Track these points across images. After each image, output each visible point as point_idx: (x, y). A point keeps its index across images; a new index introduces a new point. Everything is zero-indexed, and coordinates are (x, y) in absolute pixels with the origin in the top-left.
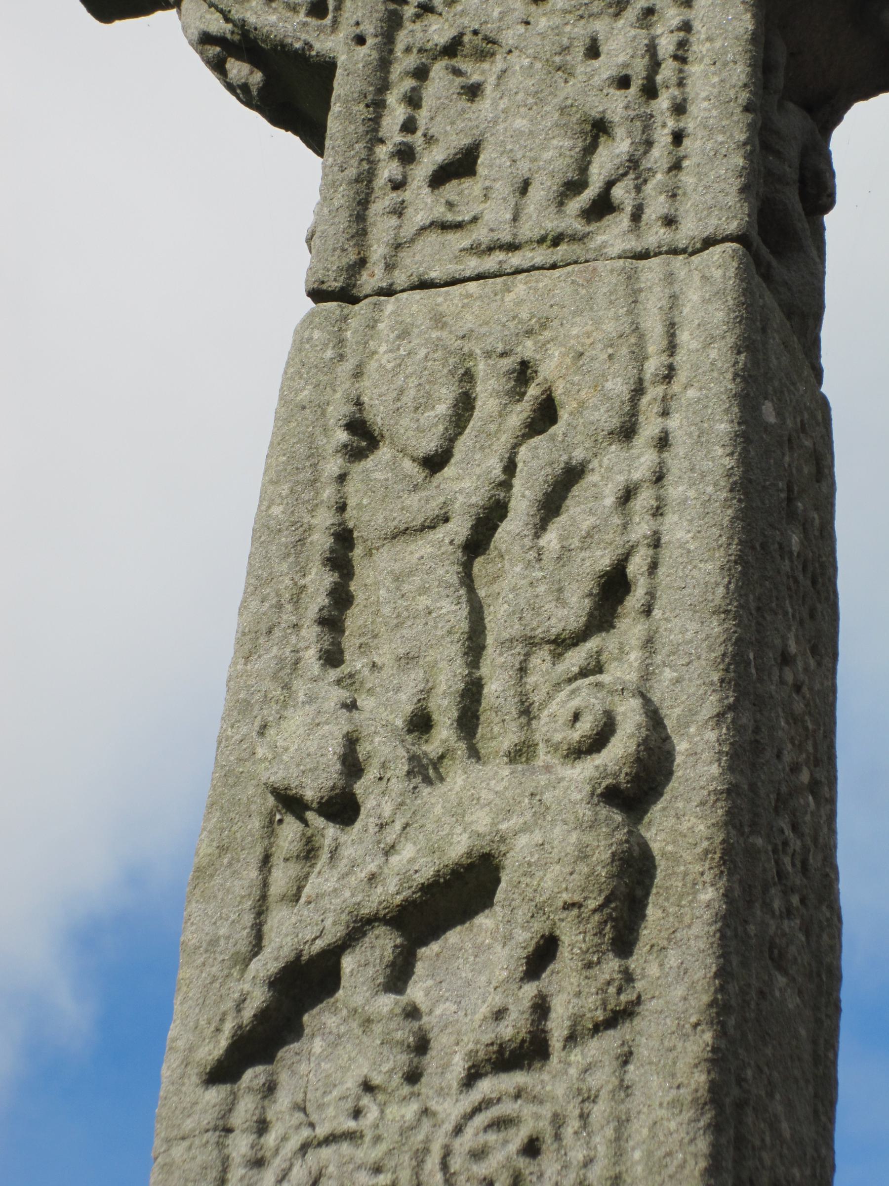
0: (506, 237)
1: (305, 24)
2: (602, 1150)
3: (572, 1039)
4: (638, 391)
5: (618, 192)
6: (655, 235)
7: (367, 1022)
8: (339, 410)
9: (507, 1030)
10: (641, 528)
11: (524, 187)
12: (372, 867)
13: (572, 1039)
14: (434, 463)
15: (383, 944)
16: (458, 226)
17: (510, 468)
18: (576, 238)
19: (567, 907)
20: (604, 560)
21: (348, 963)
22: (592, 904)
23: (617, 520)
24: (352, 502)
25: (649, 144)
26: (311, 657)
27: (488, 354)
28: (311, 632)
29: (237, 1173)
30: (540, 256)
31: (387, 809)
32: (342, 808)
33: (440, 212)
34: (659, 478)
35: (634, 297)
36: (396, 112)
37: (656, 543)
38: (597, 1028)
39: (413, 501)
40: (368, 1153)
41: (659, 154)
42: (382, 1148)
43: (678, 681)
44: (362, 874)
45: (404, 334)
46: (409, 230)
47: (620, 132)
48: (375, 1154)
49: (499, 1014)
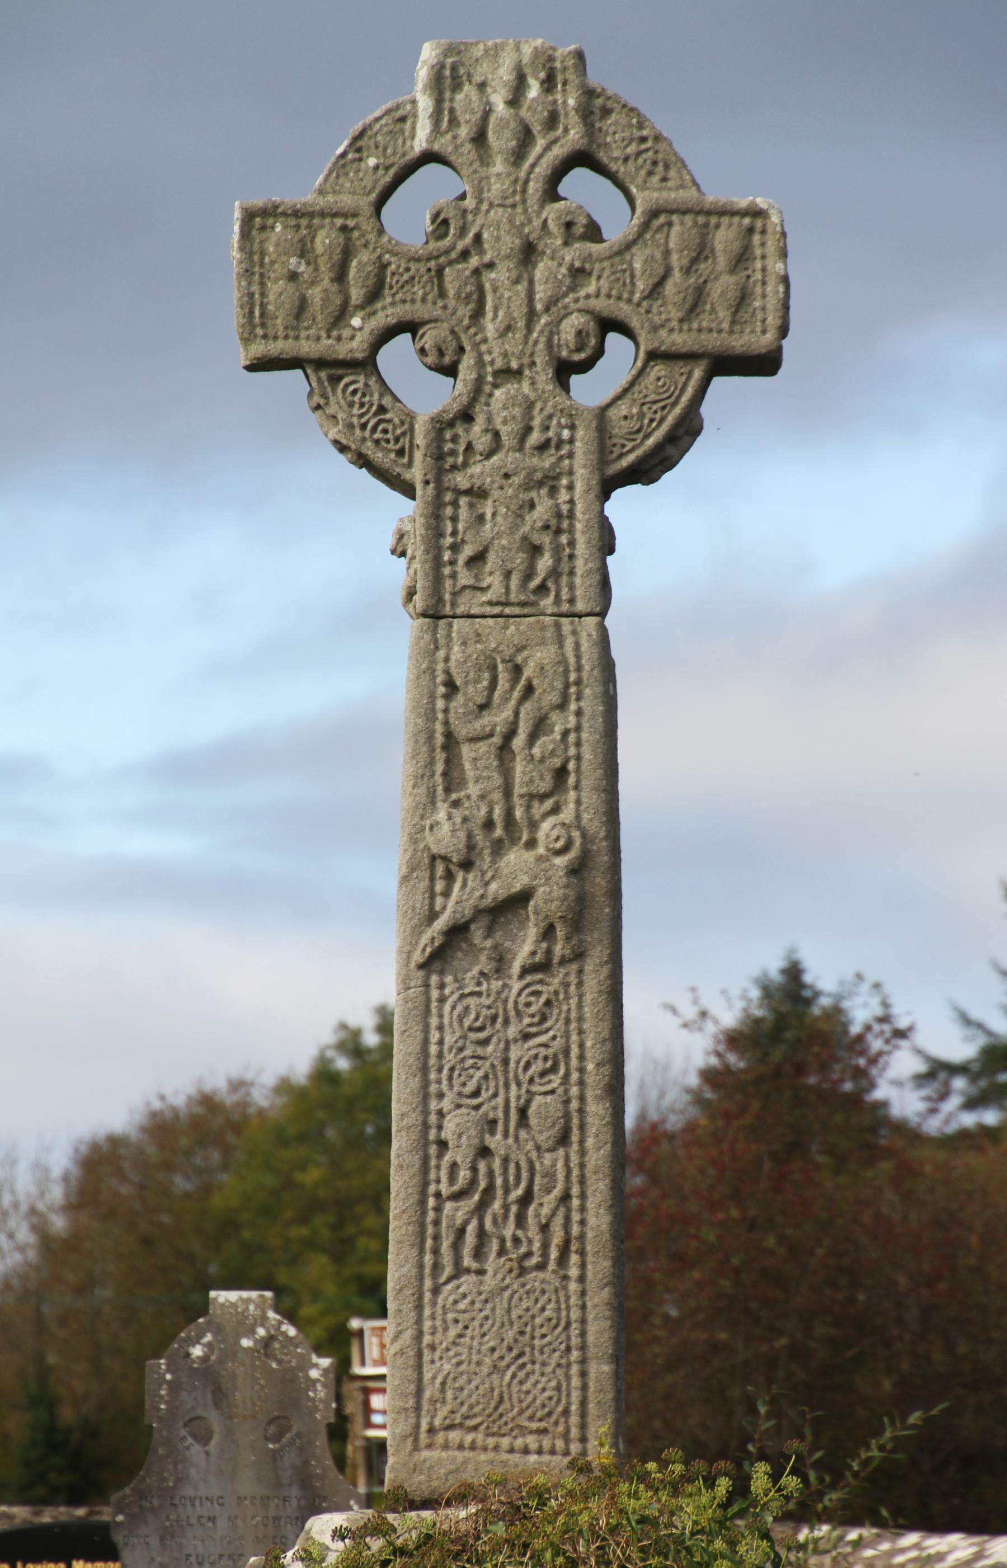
0: (503, 599)
1: (395, 461)
2: (573, 1006)
4: (567, 686)
6: (565, 607)
8: (440, 678)
9: (538, 958)
10: (572, 751)
11: (508, 575)
12: (481, 892)
14: (483, 707)
15: (485, 920)
17: (517, 714)
19: (560, 917)
20: (557, 762)
21: (473, 927)
23: (562, 747)
24: (451, 720)
26: (440, 789)
28: (438, 779)
29: (434, 1005)
30: (517, 610)
32: (467, 865)
33: (471, 581)
34: (578, 728)
36: (449, 527)
37: (578, 758)
38: (570, 961)
40: (485, 1001)
42: (492, 999)
43: (591, 820)
44: (478, 894)
45: (464, 643)
46: (457, 588)
48: (488, 1002)
49: (533, 953)
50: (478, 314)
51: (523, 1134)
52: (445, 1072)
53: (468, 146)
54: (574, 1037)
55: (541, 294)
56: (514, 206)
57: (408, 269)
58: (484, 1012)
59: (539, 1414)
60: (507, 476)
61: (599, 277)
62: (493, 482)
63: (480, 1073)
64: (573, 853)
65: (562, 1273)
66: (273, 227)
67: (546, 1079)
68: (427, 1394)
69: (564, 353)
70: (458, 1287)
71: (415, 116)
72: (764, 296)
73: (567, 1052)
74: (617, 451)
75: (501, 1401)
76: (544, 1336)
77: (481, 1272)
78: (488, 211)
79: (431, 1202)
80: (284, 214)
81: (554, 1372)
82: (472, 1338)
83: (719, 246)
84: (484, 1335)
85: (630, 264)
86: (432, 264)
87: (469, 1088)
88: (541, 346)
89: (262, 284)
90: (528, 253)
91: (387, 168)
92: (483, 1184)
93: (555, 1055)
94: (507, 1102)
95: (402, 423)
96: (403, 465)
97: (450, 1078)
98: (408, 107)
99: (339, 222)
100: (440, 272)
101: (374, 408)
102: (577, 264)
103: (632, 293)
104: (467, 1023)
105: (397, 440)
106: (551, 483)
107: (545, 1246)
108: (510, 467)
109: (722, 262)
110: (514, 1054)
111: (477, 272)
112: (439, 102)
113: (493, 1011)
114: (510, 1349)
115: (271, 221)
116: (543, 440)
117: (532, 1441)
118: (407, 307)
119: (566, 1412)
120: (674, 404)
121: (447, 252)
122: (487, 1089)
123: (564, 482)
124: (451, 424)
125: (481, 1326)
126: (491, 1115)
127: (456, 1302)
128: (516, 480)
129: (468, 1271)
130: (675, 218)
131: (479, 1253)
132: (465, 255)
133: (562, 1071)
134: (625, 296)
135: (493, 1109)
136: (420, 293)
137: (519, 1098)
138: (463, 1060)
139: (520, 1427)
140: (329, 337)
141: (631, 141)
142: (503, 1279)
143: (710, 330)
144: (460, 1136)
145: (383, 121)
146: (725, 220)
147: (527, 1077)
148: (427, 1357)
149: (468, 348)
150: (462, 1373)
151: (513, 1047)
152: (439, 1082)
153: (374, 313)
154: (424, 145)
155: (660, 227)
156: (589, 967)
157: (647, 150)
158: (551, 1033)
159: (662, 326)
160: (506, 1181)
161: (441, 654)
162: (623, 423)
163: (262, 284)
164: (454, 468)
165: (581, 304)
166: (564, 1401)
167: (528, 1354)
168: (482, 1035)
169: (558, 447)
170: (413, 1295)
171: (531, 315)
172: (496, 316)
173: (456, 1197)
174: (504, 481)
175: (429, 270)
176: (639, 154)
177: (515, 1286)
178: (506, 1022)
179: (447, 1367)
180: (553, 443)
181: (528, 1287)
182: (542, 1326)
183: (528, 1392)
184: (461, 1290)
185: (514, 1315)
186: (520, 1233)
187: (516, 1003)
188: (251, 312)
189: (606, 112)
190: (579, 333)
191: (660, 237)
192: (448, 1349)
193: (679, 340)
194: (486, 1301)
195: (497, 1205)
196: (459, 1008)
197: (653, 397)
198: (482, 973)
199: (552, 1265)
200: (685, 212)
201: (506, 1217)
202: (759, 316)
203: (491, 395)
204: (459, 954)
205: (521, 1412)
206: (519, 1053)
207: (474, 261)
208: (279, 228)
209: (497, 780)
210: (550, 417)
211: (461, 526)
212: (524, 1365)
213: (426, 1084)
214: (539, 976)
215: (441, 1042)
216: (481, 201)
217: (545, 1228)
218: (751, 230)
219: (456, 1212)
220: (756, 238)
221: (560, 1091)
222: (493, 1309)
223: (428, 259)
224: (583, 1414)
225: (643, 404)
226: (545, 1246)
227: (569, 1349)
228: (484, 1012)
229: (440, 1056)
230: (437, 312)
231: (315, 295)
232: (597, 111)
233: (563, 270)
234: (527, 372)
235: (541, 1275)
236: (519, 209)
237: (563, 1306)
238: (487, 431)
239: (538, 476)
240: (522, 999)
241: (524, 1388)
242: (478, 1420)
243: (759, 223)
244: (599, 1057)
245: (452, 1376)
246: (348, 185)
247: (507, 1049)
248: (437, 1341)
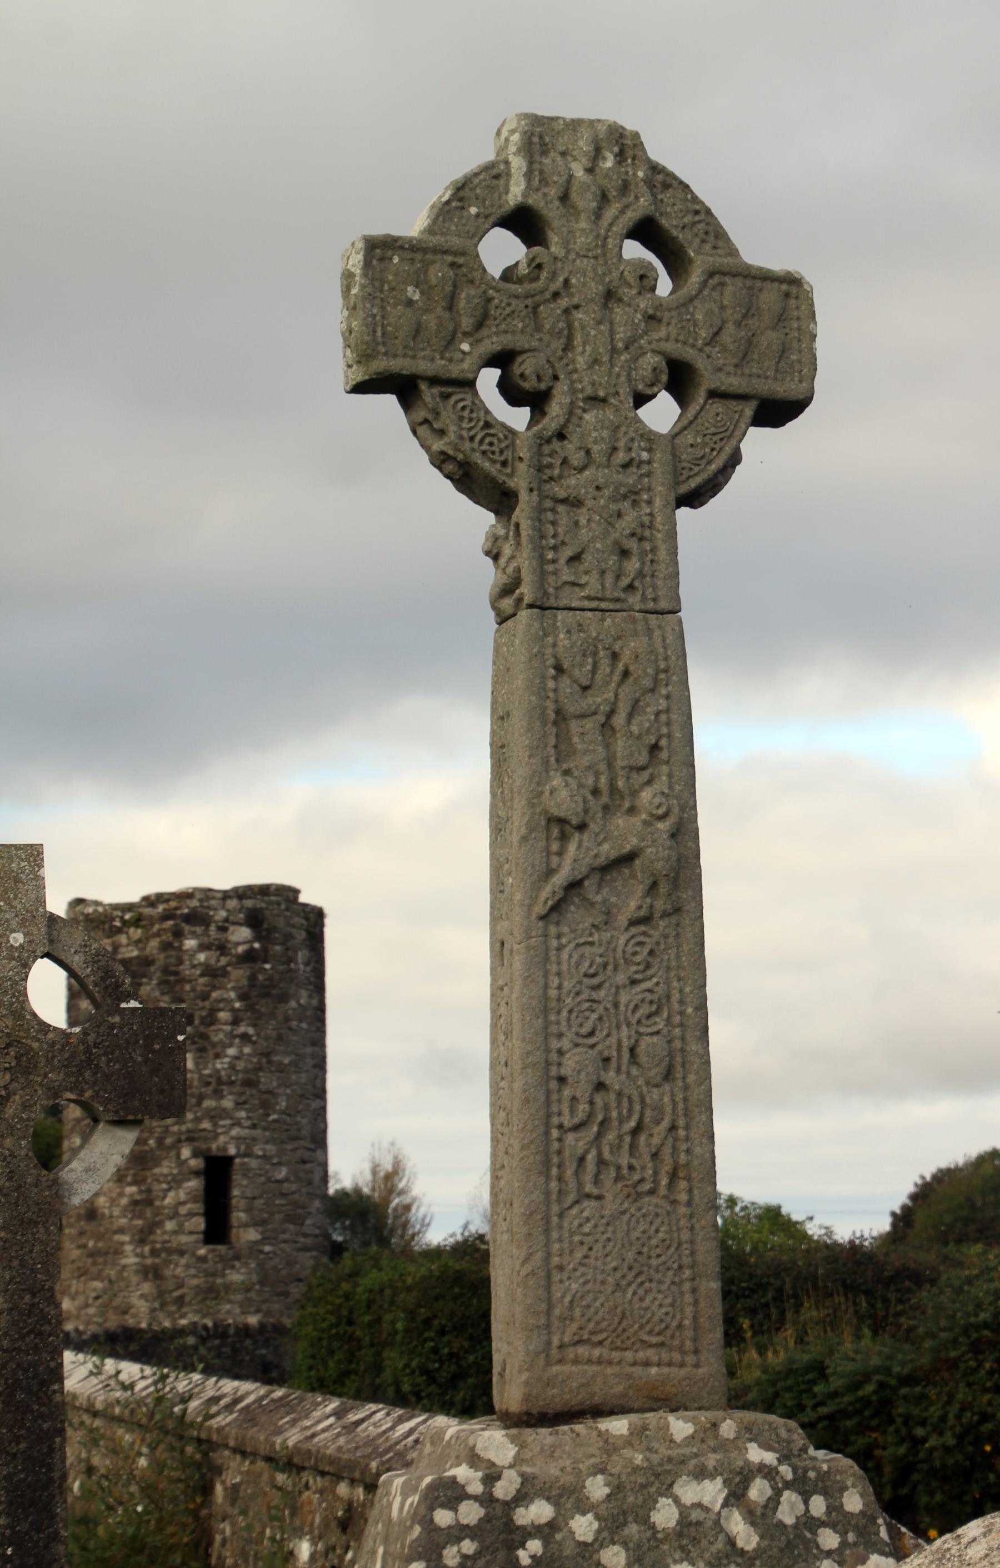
0: (599, 595)
2: (673, 956)
5: (637, 583)
6: (651, 605)
8: (551, 661)
9: (642, 913)
11: (603, 573)
17: (616, 695)
21: (586, 883)
27: (605, 648)
28: (552, 751)
32: (582, 827)
33: (572, 578)
35: (649, 632)
37: (669, 736)
38: (670, 914)
45: (569, 632)
46: (559, 584)
48: (601, 951)
49: (640, 907)
50: (568, 347)
52: (564, 1013)
53: (557, 203)
55: (622, 334)
56: (596, 258)
57: (509, 305)
58: (599, 960)
59: (657, 1329)
60: (598, 488)
61: (669, 324)
62: (587, 493)
63: (594, 1016)
66: (391, 259)
68: (557, 1312)
69: (640, 387)
70: (582, 1212)
71: (509, 175)
73: (668, 997)
74: (686, 474)
75: (622, 1319)
76: (659, 1256)
79: (555, 1133)
80: (402, 248)
81: (669, 1288)
82: (597, 1259)
84: (606, 1256)
85: (693, 315)
86: (529, 302)
88: (623, 379)
89: (383, 308)
91: (487, 217)
93: (659, 999)
95: (506, 437)
96: (507, 475)
98: (502, 167)
99: (450, 259)
100: (535, 308)
101: (481, 423)
102: (650, 311)
103: (696, 339)
105: (501, 452)
106: (633, 497)
108: (601, 481)
110: (624, 998)
111: (567, 311)
112: (531, 163)
114: (630, 1268)
115: (390, 253)
116: (627, 459)
117: (650, 1354)
118: (509, 337)
121: (542, 292)
124: (549, 441)
125: (604, 1247)
126: (606, 1054)
127: (581, 1225)
128: (606, 492)
129: (588, 1196)
130: (727, 279)
132: (556, 295)
133: (665, 1015)
136: (520, 325)
137: (630, 1037)
138: (579, 1003)
139: (643, 1341)
140: (442, 358)
141: (688, 212)
143: (759, 376)
144: (579, 1072)
145: (481, 177)
146: (768, 285)
148: (556, 1277)
149: (562, 376)
150: (589, 1292)
151: (622, 992)
152: (558, 1023)
153: (480, 341)
154: (520, 199)
155: (714, 288)
157: (700, 222)
158: (655, 980)
160: (620, 1113)
161: (550, 640)
162: (690, 450)
163: (383, 308)
165: (654, 346)
166: (678, 1317)
168: (595, 981)
171: (614, 351)
172: (584, 352)
173: (576, 1128)
174: (596, 493)
176: (694, 224)
178: (616, 968)
179: (575, 1286)
180: (635, 463)
183: (647, 1309)
184: (585, 1214)
187: (624, 952)
189: (666, 186)
190: (655, 369)
191: (716, 294)
192: (575, 1270)
193: (733, 382)
194: (608, 1224)
195: (611, 1136)
196: (576, 957)
197: (713, 430)
199: (663, 1191)
201: (619, 1147)
202: (797, 367)
204: (572, 908)
205: (642, 1327)
206: (628, 998)
207: (564, 302)
210: (632, 440)
212: (642, 1283)
214: (642, 928)
215: (560, 987)
218: (787, 295)
219: (575, 1143)
222: (614, 1232)
223: (526, 297)
224: (696, 1328)
228: (599, 960)
230: (535, 344)
231: (430, 320)
232: (659, 185)
233: (639, 316)
235: (654, 1200)
236: (601, 261)
237: (675, 1228)
238: (580, 448)
239: (623, 490)
240: (630, 949)
241: (644, 1305)
243: (794, 290)
246: (453, 228)
247: (617, 993)
248: (565, 1263)
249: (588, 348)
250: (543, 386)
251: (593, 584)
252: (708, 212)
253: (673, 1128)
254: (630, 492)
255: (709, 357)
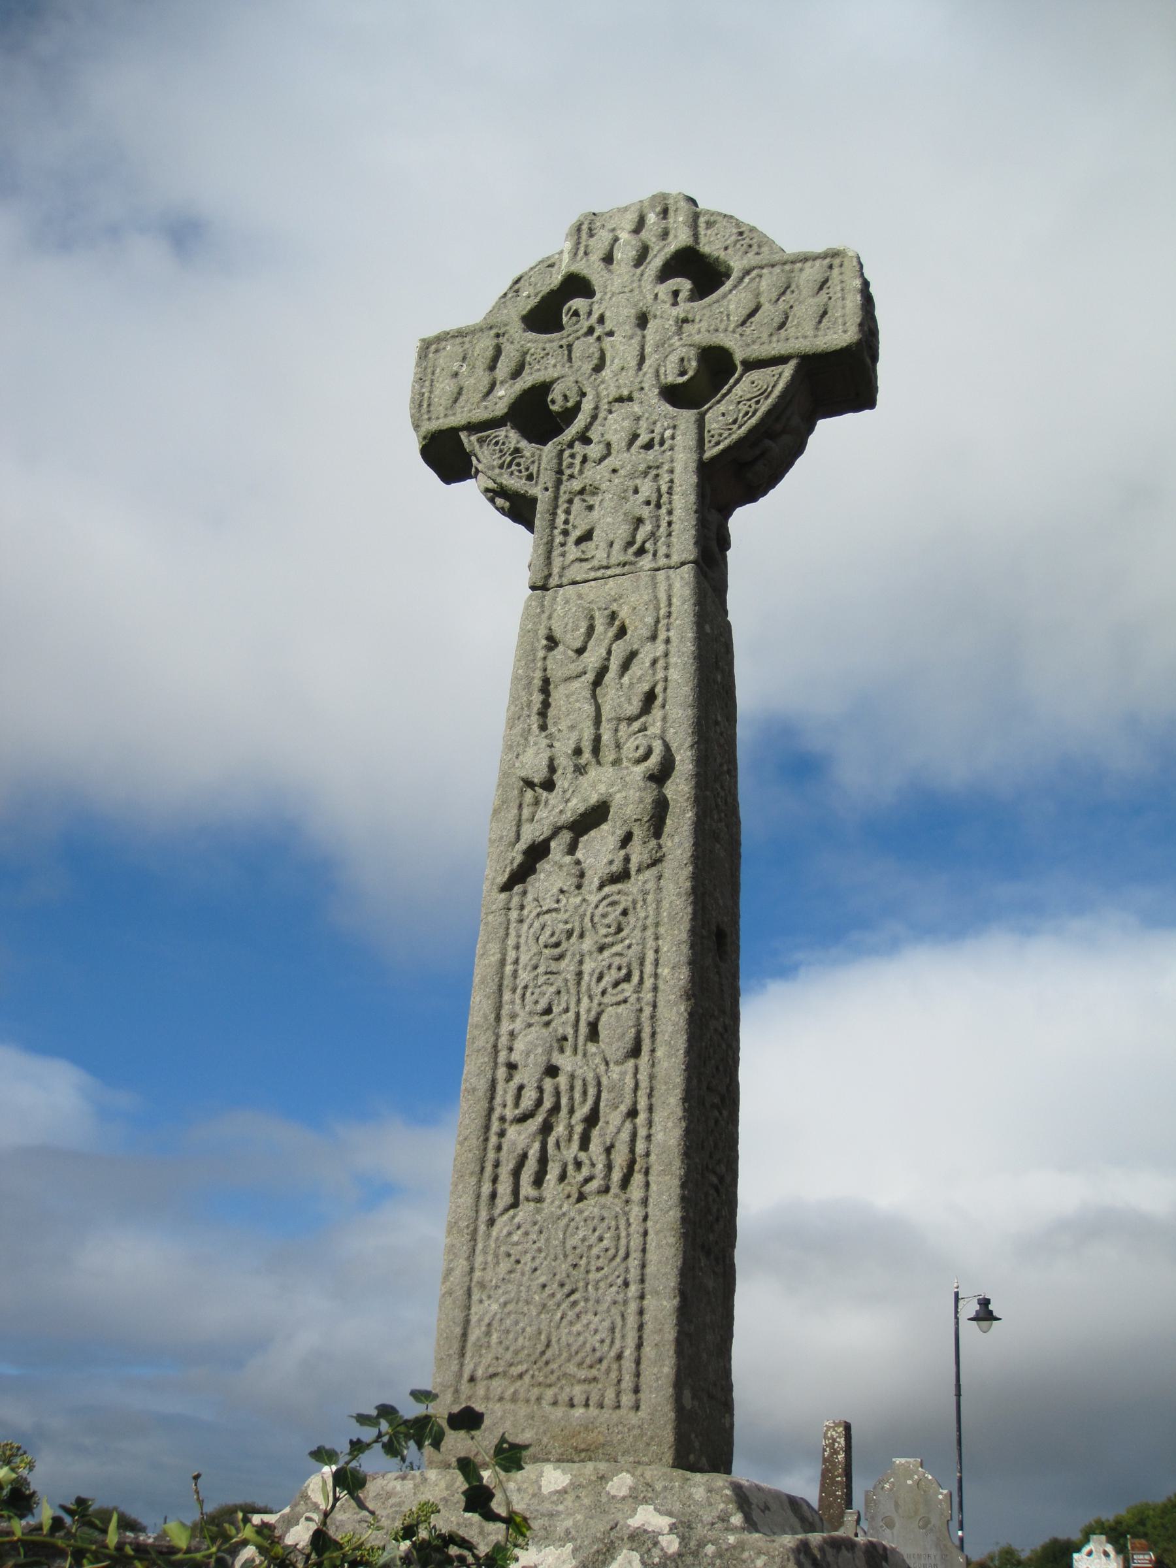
0: (605, 563)
3: (639, 871)
4: (657, 622)
5: (647, 545)
6: (662, 561)
7: (561, 867)
8: (542, 632)
9: (614, 868)
10: (660, 675)
11: (611, 544)
12: (561, 808)
13: (639, 871)
14: (580, 651)
15: (566, 836)
16: (587, 560)
17: (609, 652)
18: (632, 563)
19: (636, 820)
20: (646, 687)
21: (553, 844)
22: (645, 819)
24: (549, 667)
25: (659, 526)
26: (535, 727)
27: (599, 609)
29: (513, 925)
30: (618, 570)
31: (566, 785)
32: (549, 785)
33: (579, 555)
34: (666, 655)
35: (655, 586)
36: (561, 517)
37: (666, 680)
38: (649, 866)
39: (572, 666)
40: (563, 916)
41: (663, 530)
42: (568, 914)
45: (567, 602)
46: (567, 562)
47: (647, 522)
48: (566, 916)
49: (611, 862)
51: (592, 1048)
52: (519, 991)
54: (651, 943)
58: (561, 926)
59: (588, 1361)
60: (614, 471)
63: (553, 989)
64: (654, 759)
65: (624, 1197)
67: (620, 988)
68: (472, 1338)
70: (513, 1217)
72: (844, 308)
75: (548, 1345)
76: (599, 1269)
77: (539, 1200)
78: (610, 298)
79: (495, 1126)
81: (608, 1310)
82: (523, 1274)
83: (802, 282)
84: (535, 1270)
87: (543, 1004)
90: (642, 320)
92: (548, 1104)
94: (578, 1015)
97: (523, 996)
99: (493, 332)
102: (682, 316)
103: (728, 326)
104: (542, 939)
105: (527, 469)
106: (654, 472)
107: (609, 1167)
108: (617, 465)
109: (805, 292)
110: (587, 967)
111: (599, 339)
113: (569, 926)
118: (542, 373)
119: (619, 1357)
120: (767, 398)
122: (559, 1004)
123: (666, 467)
125: (534, 1259)
126: (561, 1031)
127: (510, 1234)
128: (622, 472)
130: (765, 271)
131: (538, 1181)
132: (591, 331)
133: (635, 979)
134: (722, 327)
135: (562, 1024)
137: (589, 1011)
142: (560, 1207)
144: (528, 1055)
146: (809, 264)
147: (600, 990)
150: (509, 1313)
151: (587, 959)
152: (513, 1002)
156: (667, 867)
158: (627, 942)
159: (754, 342)
160: (571, 1098)
162: (721, 418)
164: (572, 476)
166: (618, 1344)
167: (581, 1289)
168: (557, 951)
169: (662, 443)
170: (467, 1227)
171: (642, 359)
175: (561, 347)
177: (572, 1214)
178: (582, 936)
180: (657, 441)
181: (586, 1214)
182: (598, 1257)
183: (579, 1334)
185: (570, 1242)
186: (582, 1156)
188: (420, 405)
190: (682, 360)
192: (497, 1287)
197: (749, 396)
198: (562, 891)
199: (615, 1189)
200: (773, 266)
201: (570, 1140)
202: (840, 321)
203: (605, 419)
206: (593, 965)
208: (449, 348)
209: (589, 709)
210: (654, 423)
211: (571, 517)
212: (575, 1303)
213: (499, 1007)
214: (619, 886)
215: (516, 962)
216: (605, 293)
217: (608, 1150)
218: (831, 267)
219: (520, 1137)
220: (836, 271)
221: (632, 999)
225: (739, 403)
226: (609, 1167)
227: (626, 1284)
228: (561, 926)
229: (515, 974)
231: (469, 383)
234: (636, 395)
235: (603, 1199)
237: (623, 1234)
239: (642, 467)
241: (575, 1329)
242: (525, 1367)
243: (837, 262)
244: (674, 959)
245: (498, 1316)
247: (581, 962)
248: (488, 1278)
249: (616, 361)
250: (570, 404)
251: (600, 556)
252: (753, 229)
253: (633, 1113)
254: (650, 468)
255: (741, 335)
